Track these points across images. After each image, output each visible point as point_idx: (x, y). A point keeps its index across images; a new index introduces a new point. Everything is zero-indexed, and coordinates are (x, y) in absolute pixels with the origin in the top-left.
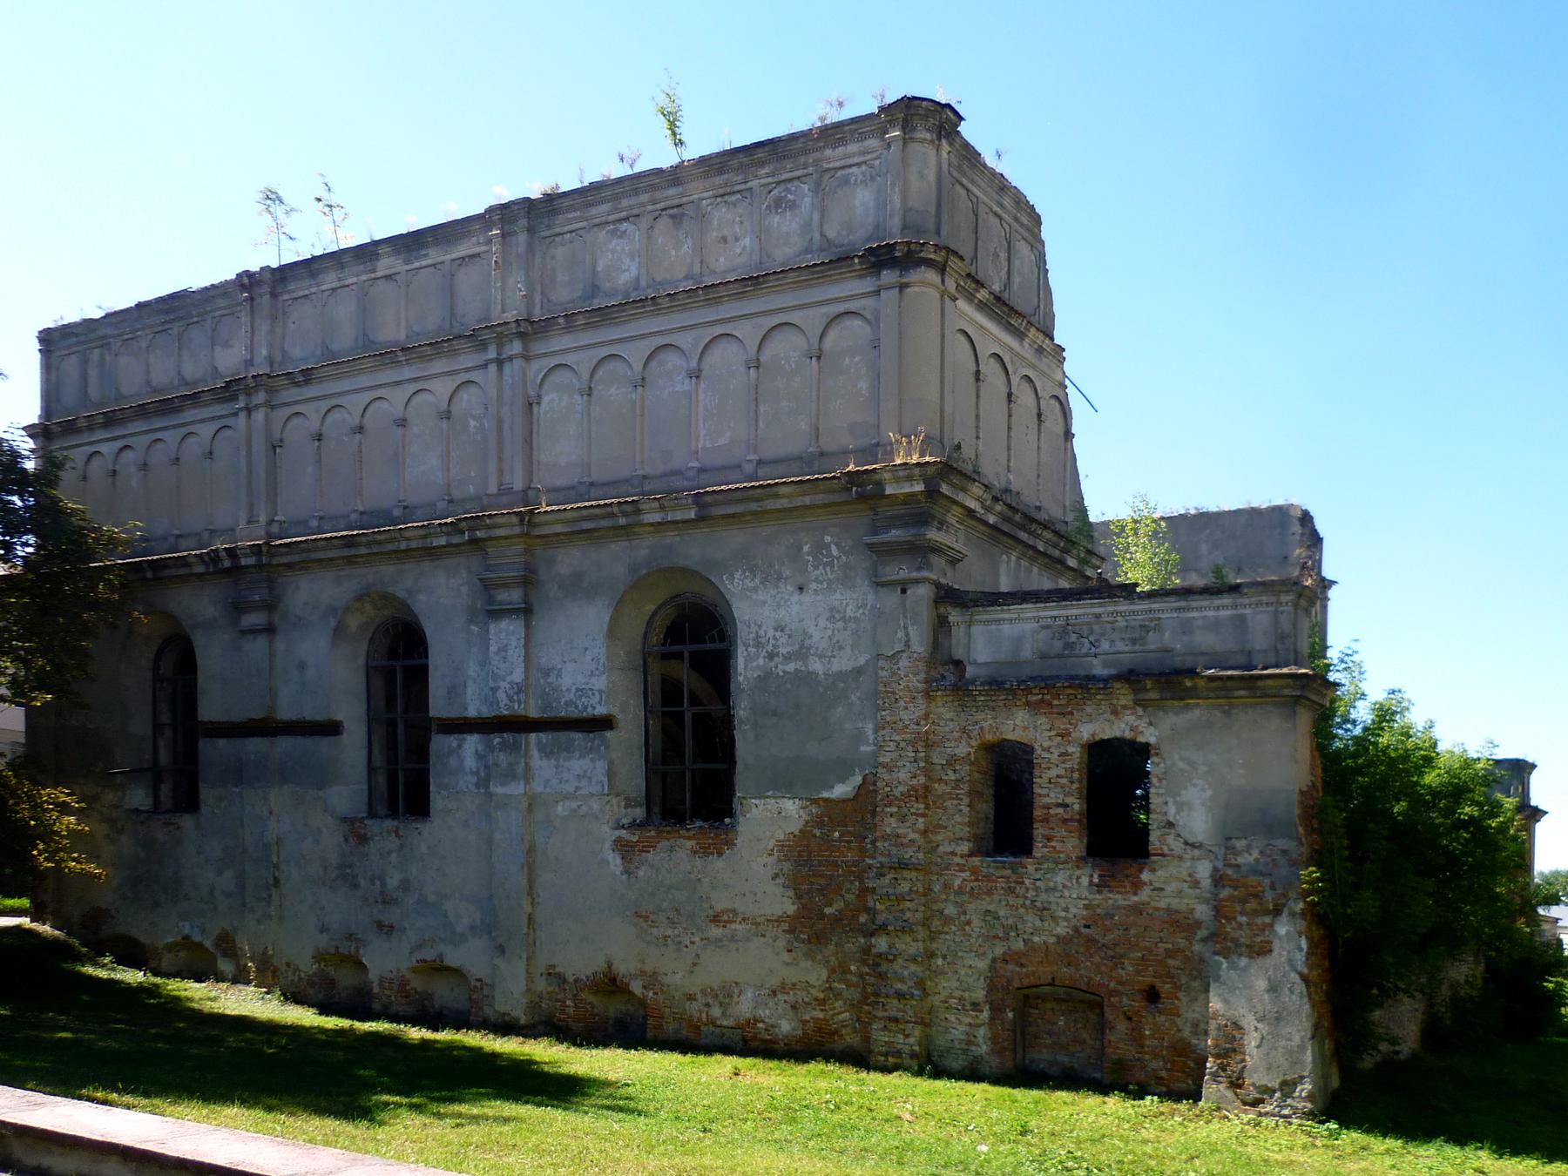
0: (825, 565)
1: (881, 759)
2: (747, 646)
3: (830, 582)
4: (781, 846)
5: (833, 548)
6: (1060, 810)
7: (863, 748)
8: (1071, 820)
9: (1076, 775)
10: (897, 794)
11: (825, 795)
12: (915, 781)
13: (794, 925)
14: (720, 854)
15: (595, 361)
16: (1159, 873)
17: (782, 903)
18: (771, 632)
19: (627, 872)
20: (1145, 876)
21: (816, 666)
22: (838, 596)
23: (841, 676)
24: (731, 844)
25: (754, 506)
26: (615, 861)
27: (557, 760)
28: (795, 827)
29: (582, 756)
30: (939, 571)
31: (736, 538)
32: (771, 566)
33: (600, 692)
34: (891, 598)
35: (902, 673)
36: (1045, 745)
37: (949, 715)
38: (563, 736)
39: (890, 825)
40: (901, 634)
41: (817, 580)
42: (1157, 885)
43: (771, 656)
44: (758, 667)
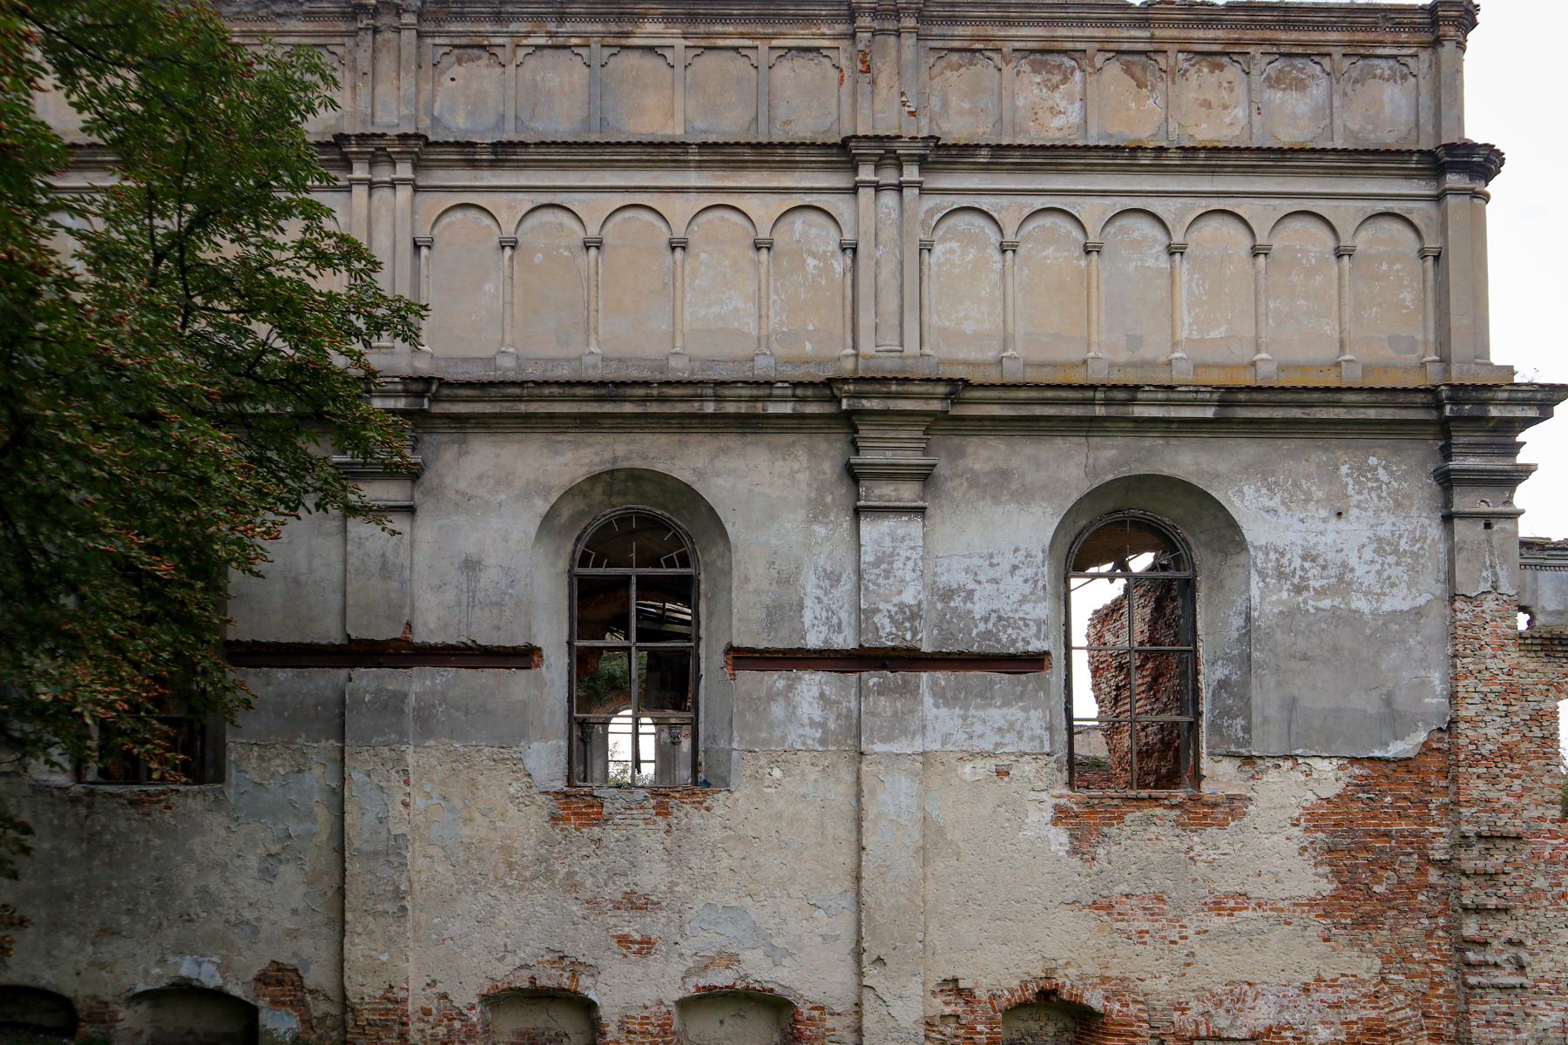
2: (1263, 575)
10: (1484, 752)
11: (1377, 753)
12: (1507, 738)
13: (1325, 907)
14: (1222, 825)
15: (1027, 212)
17: (1314, 882)
18: (1297, 562)
19: (1074, 851)
21: (1360, 603)
26: (1059, 838)
27: (965, 707)
28: (1331, 790)
29: (1003, 705)
31: (1248, 450)
32: (1296, 485)
33: (1039, 623)
37: (1532, 666)
38: (974, 676)
41: (1358, 506)
43: (1298, 590)
44: (1280, 602)
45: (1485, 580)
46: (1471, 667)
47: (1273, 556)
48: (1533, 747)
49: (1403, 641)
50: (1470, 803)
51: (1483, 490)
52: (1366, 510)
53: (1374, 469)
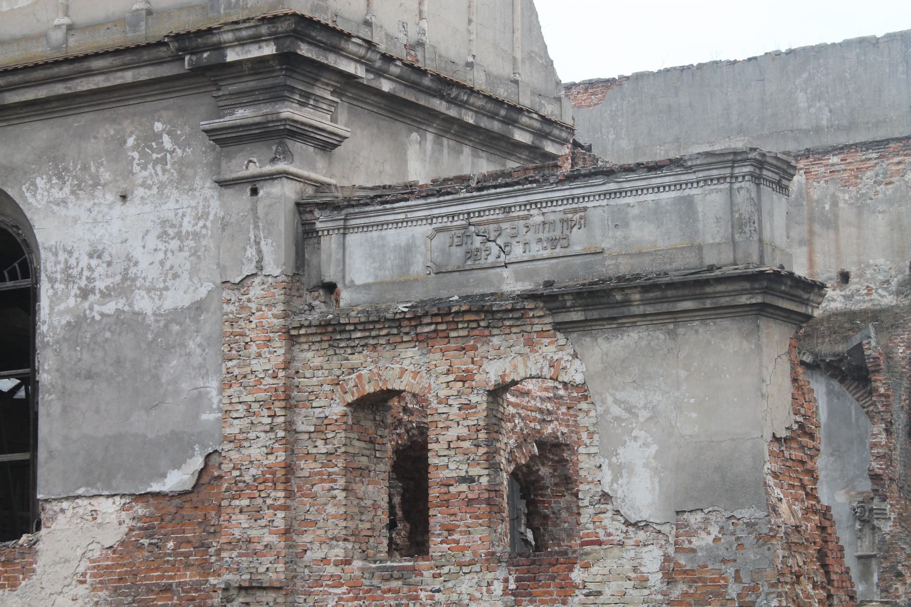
0: (156, 162)
1: (228, 431)
2: (52, 281)
3: (162, 186)
4: (98, 569)
5: (166, 139)
6: (464, 487)
7: (205, 417)
8: (477, 500)
9: (482, 435)
10: (248, 478)
11: (155, 487)
12: (272, 458)
16: (594, 570)
18: (84, 261)
20: (577, 575)
21: (144, 303)
22: (171, 204)
23: (176, 315)
24: (28, 571)
25: (60, 89)
28: (113, 536)
30: (307, 164)
31: (39, 134)
32: (85, 168)
34: (240, 200)
35: (253, 306)
36: (443, 393)
37: (317, 361)
39: (239, 525)
40: (251, 252)
41: (143, 185)
42: (592, 587)
43: (85, 293)
44: (68, 311)
45: (250, 260)
46: (236, 371)
47: (62, 256)
48: (317, 467)
49: (183, 345)
50: (232, 544)
51: (248, 147)
52: (150, 188)
53: (158, 137)
